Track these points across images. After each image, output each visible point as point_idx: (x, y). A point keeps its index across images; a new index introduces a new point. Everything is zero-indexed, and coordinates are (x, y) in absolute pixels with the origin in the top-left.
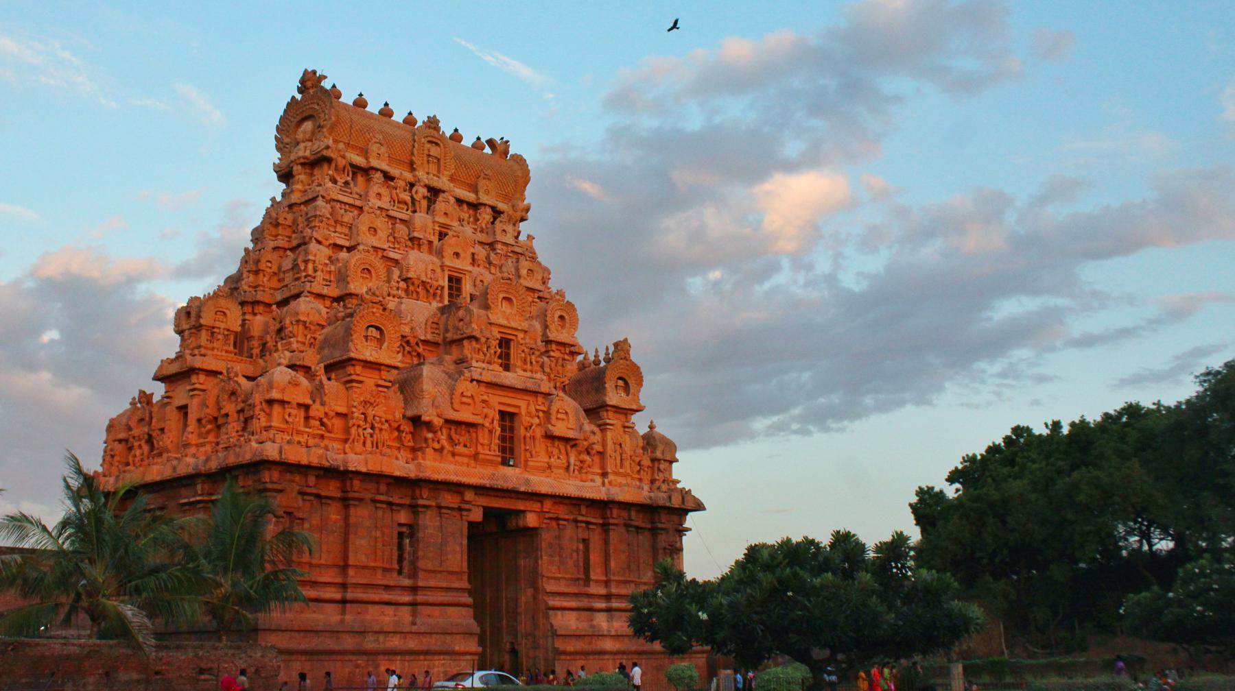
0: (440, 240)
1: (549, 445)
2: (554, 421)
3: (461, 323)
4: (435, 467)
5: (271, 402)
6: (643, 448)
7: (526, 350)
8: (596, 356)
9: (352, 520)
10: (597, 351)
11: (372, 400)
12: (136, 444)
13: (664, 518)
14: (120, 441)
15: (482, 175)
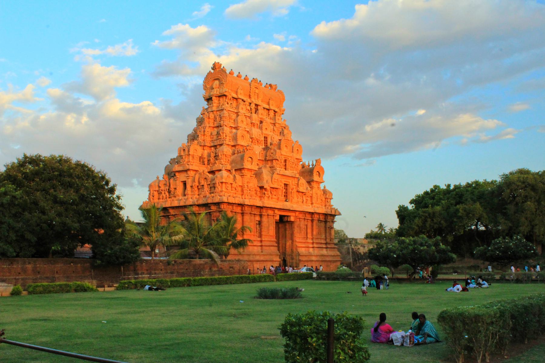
0: (260, 123)
1: (298, 194)
2: (299, 186)
3: (272, 154)
4: (268, 202)
5: (222, 183)
6: (323, 195)
7: (292, 163)
8: (309, 163)
9: (245, 220)
10: (309, 162)
11: (250, 181)
12: (163, 192)
13: (329, 217)
14: (155, 191)
15: (271, 99)
